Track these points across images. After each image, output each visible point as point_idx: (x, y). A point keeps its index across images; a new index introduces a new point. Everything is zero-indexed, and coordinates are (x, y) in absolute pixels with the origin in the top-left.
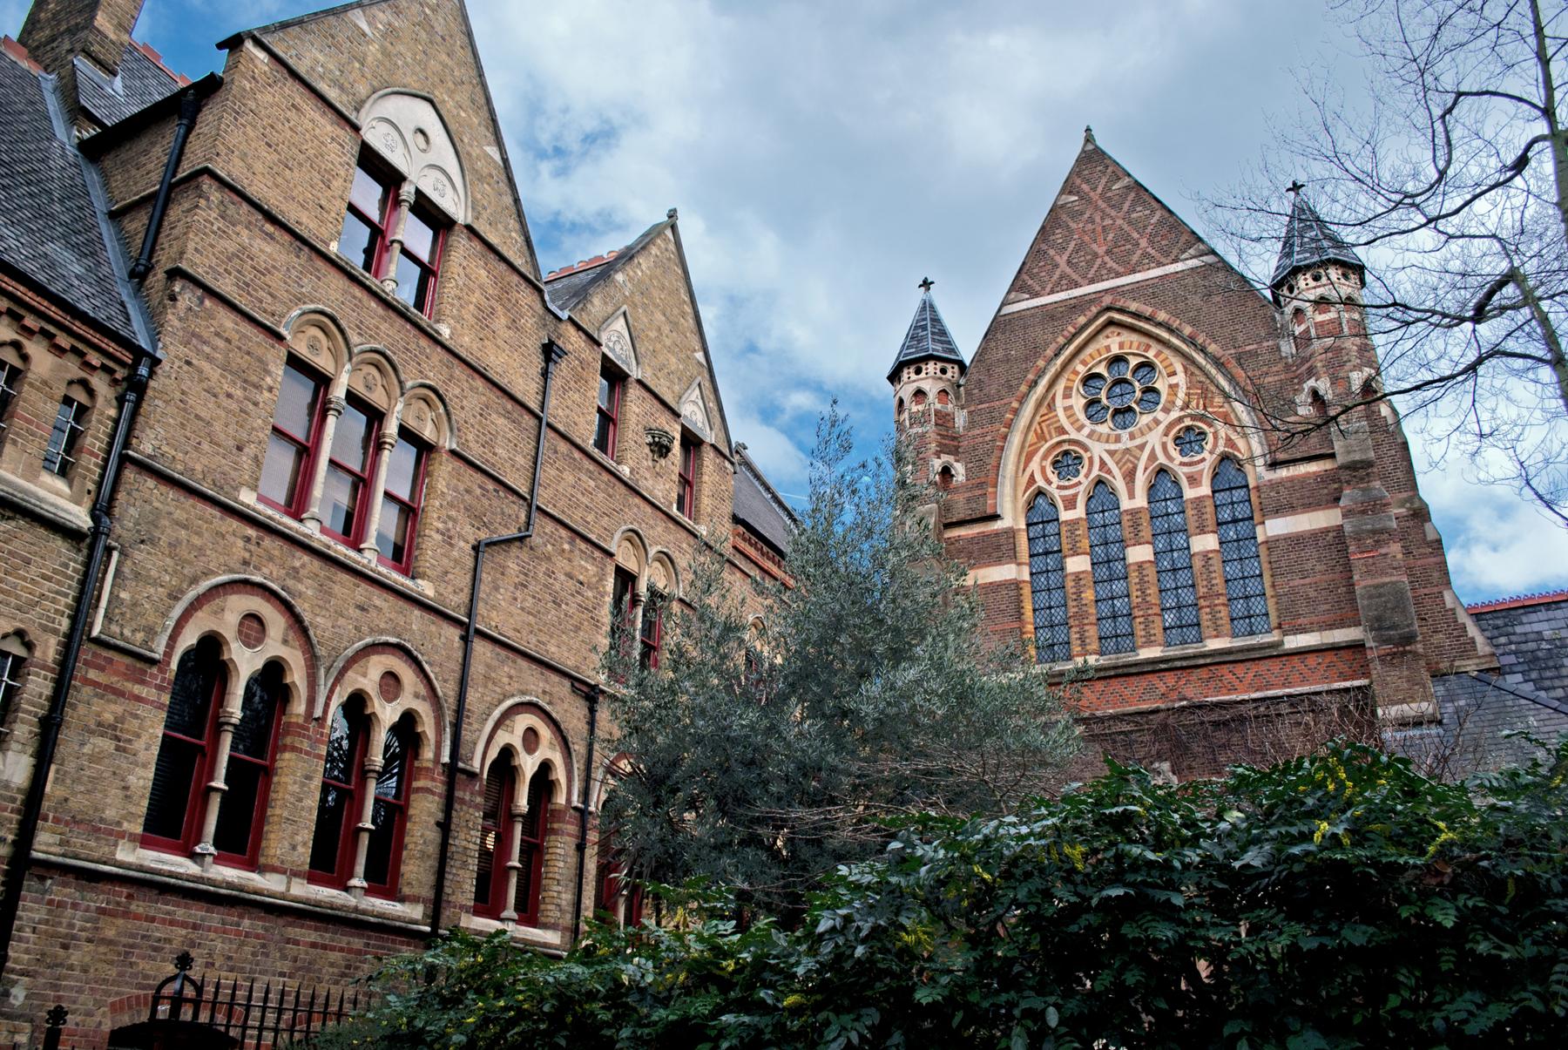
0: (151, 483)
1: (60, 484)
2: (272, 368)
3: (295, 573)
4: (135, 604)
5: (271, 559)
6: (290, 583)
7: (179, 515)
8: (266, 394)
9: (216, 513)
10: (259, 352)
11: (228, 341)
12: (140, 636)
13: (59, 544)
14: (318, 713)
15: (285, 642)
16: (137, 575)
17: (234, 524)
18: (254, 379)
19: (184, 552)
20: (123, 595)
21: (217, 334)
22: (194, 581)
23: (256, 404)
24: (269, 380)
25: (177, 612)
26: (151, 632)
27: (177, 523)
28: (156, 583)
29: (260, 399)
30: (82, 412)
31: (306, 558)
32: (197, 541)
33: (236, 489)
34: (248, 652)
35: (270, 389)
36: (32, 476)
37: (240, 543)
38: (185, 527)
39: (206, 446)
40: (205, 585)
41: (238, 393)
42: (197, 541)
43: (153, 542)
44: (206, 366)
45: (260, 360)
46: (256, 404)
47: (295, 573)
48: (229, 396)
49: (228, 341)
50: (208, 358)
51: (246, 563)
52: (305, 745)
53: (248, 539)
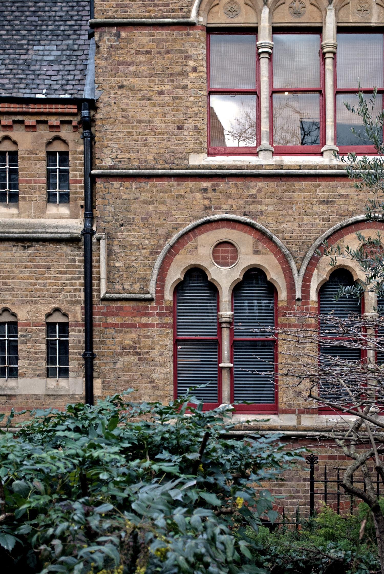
0: (116, 184)
1: (64, 210)
2: (192, 52)
3: (254, 199)
4: (128, 267)
5: (228, 197)
6: (250, 208)
7: (143, 196)
8: (192, 75)
9: (173, 182)
10: (177, 46)
11: (148, 52)
12: (137, 287)
13: (65, 249)
14: (298, 295)
15: (256, 252)
16: (124, 248)
17: (190, 184)
18: (178, 69)
19: (154, 220)
20: (117, 264)
21: (138, 53)
22: (168, 236)
23: (185, 88)
24: (191, 63)
25: (158, 263)
26: (145, 281)
27: (144, 202)
28: (139, 248)
29: (186, 81)
30: (64, 156)
31: (261, 184)
32: (162, 208)
33: (186, 158)
34: (225, 270)
35: (195, 69)
36: (42, 213)
37: (199, 196)
38: (151, 203)
39: (152, 139)
40: (176, 236)
41: (168, 87)
42: (162, 208)
43: (130, 222)
44: (136, 82)
45: (180, 52)
46: (185, 88)
47: (254, 199)
48: (161, 93)
49: (148, 52)
50: (135, 75)
51: (207, 208)
52: (293, 321)
53: (205, 190)
